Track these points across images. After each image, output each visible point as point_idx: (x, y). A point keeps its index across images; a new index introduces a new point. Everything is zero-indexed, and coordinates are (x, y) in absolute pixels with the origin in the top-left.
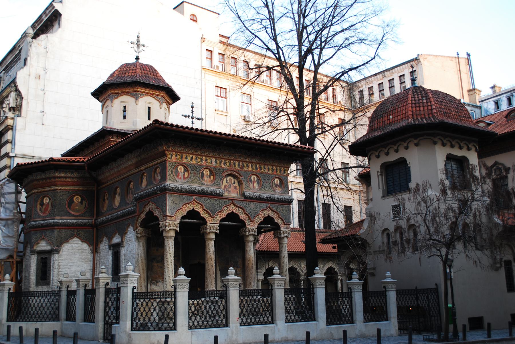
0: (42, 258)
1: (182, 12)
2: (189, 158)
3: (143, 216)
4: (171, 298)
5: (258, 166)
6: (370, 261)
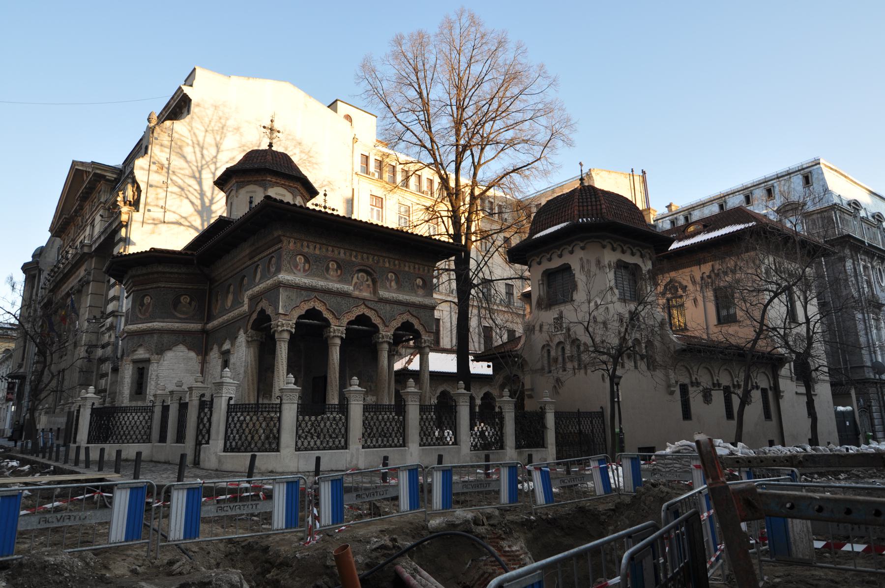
0: (139, 368)
1: (335, 111)
2: (311, 247)
3: (254, 316)
4: (276, 412)
5: (397, 262)
6: (527, 381)
